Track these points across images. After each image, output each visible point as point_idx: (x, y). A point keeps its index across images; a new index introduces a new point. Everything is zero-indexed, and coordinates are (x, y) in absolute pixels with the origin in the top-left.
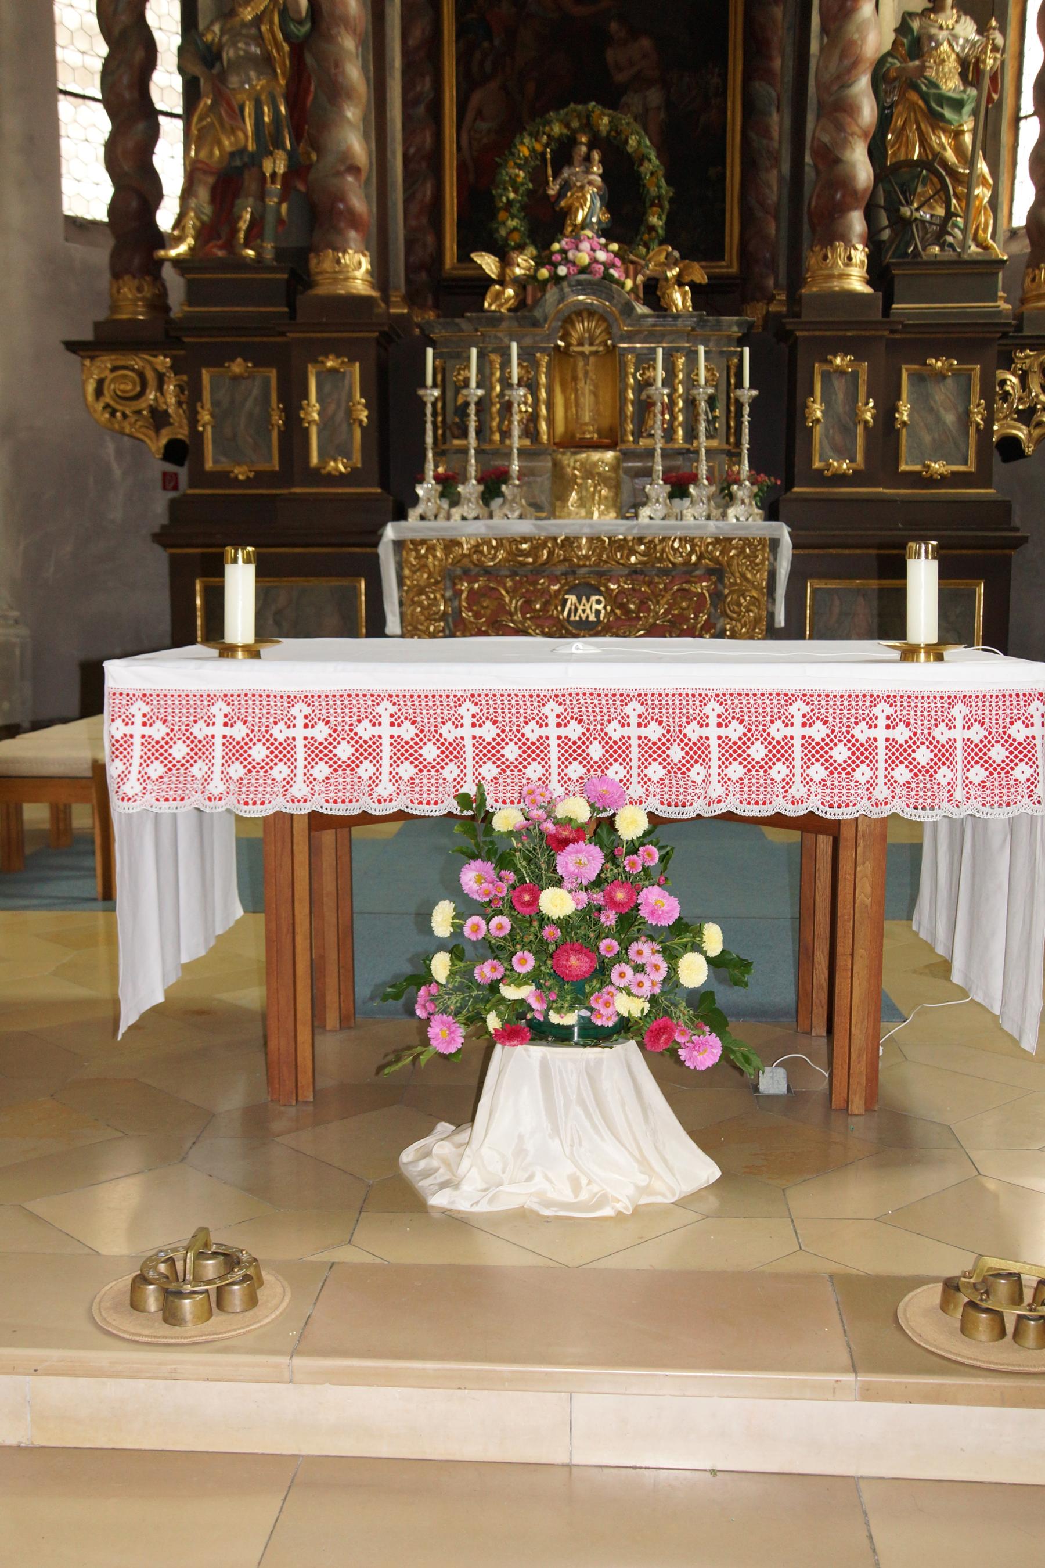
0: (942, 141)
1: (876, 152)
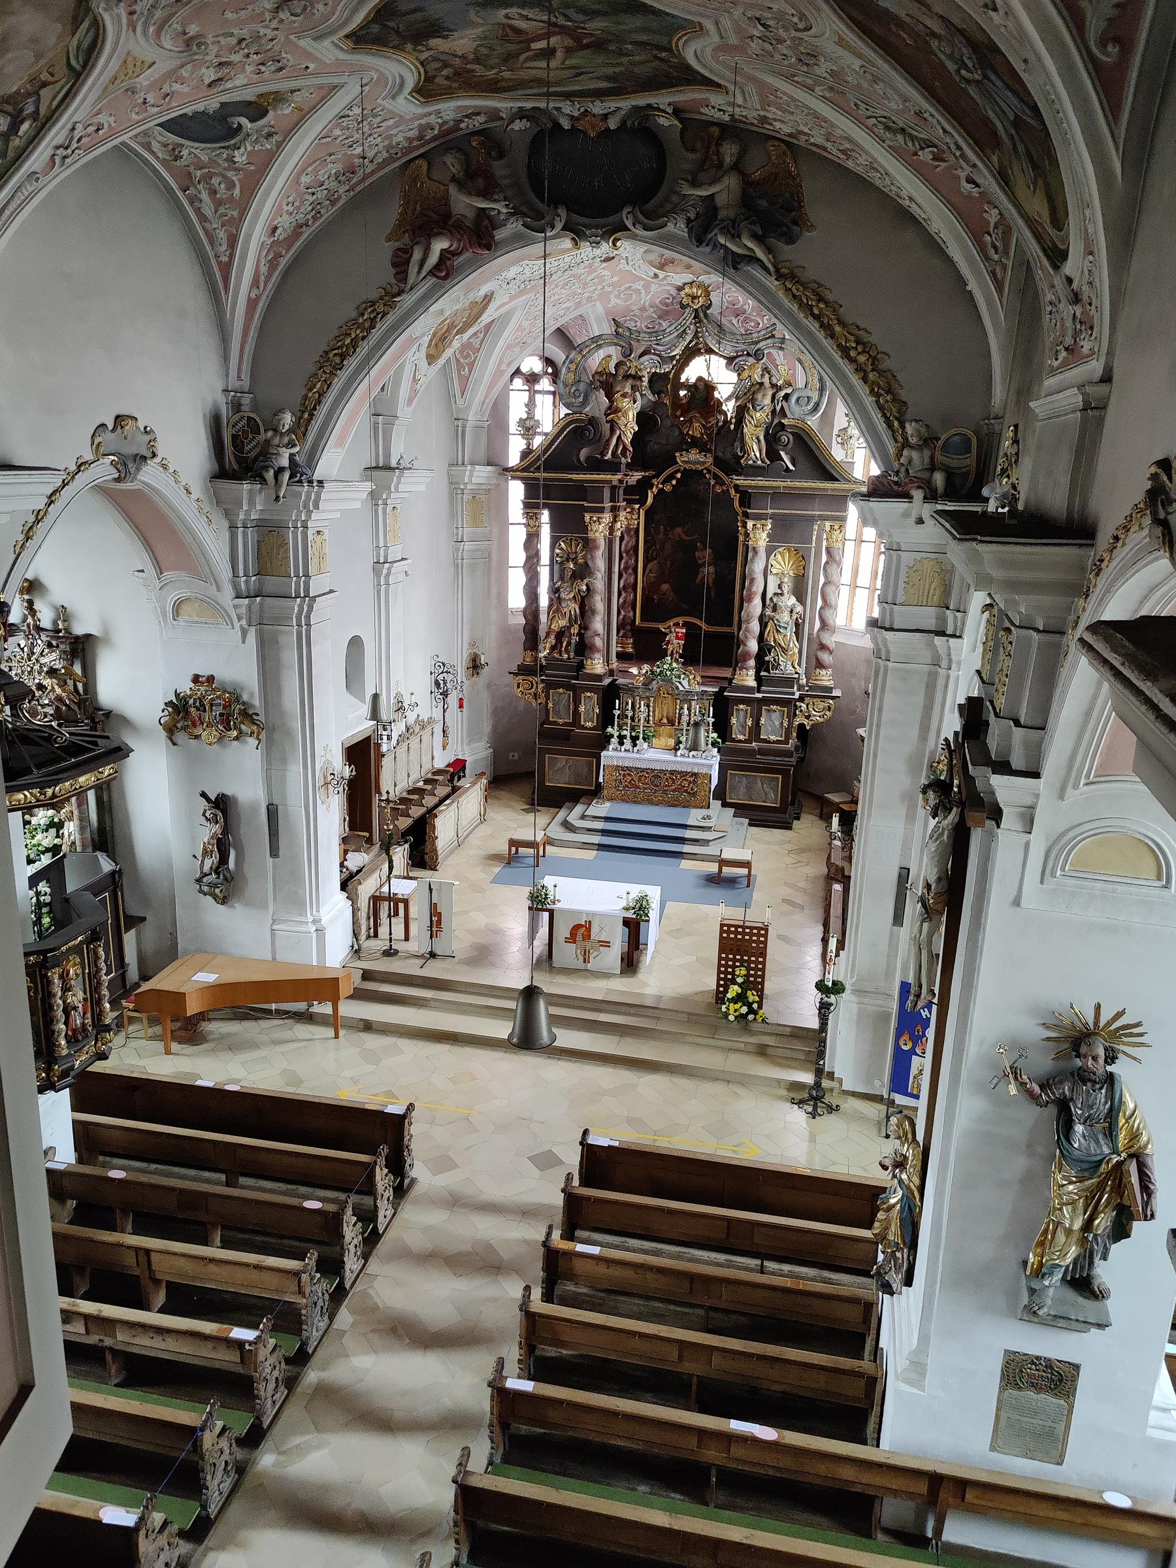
0: (779, 638)
1: (761, 639)
